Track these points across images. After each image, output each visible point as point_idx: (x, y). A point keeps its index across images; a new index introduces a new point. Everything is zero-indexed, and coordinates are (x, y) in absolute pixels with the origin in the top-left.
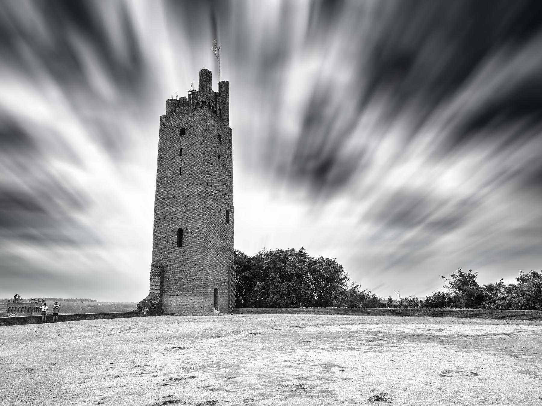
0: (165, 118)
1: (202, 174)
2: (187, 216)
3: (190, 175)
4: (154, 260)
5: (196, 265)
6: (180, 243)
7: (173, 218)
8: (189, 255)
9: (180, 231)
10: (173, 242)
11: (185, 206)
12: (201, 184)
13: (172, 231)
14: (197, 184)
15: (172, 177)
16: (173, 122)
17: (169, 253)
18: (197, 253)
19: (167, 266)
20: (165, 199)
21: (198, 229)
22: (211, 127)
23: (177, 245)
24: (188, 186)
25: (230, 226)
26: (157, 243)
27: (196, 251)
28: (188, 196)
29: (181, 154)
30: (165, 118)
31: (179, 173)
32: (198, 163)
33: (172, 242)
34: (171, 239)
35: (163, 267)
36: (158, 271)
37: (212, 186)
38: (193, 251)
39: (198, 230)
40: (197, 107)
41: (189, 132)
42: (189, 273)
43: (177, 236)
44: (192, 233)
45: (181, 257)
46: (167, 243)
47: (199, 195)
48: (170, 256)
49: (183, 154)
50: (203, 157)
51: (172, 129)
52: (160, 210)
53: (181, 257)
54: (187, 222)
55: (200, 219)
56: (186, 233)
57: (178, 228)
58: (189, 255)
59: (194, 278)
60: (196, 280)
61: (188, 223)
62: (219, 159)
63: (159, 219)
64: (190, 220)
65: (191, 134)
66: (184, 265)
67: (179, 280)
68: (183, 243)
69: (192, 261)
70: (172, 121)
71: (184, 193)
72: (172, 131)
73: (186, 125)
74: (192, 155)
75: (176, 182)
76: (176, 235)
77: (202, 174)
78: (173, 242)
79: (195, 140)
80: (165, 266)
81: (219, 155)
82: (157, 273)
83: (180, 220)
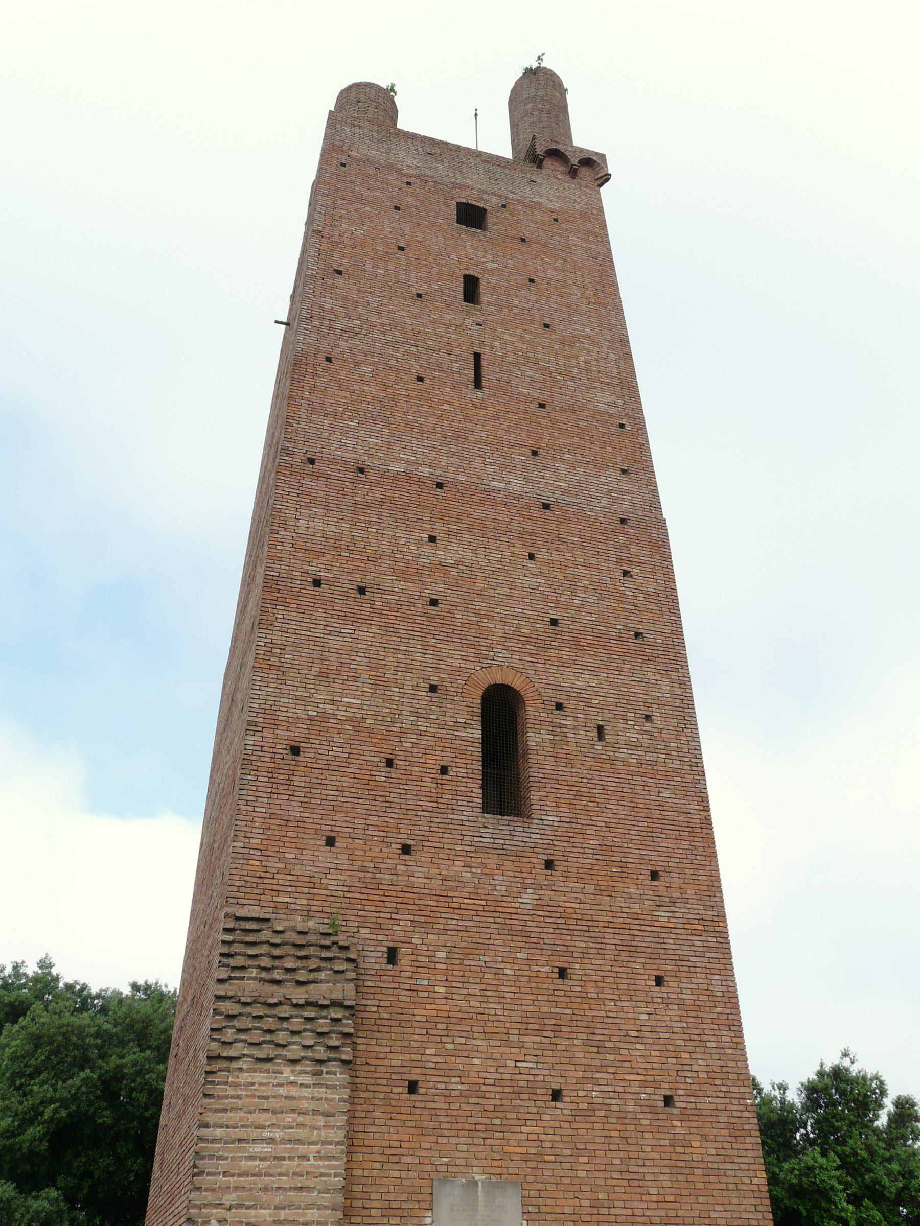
2: (554, 622)
5: (671, 984)
7: (434, 603)
8: (599, 891)
10: (444, 770)
13: (433, 688)
17: (406, 849)
18: (663, 891)
19: (392, 955)
20: (372, 476)
26: (295, 751)
31: (471, 374)
33: (433, 763)
34: (427, 742)
38: (623, 865)
39: (647, 726)
42: (616, 1051)
43: (478, 734)
45: (528, 898)
53: (528, 898)
55: (652, 659)
57: (488, 678)
58: (599, 891)
59: (668, 1101)
60: (685, 1116)
61: (562, 664)
63: (317, 583)
66: (562, 973)
68: (535, 796)
76: (465, 726)
78: (444, 770)
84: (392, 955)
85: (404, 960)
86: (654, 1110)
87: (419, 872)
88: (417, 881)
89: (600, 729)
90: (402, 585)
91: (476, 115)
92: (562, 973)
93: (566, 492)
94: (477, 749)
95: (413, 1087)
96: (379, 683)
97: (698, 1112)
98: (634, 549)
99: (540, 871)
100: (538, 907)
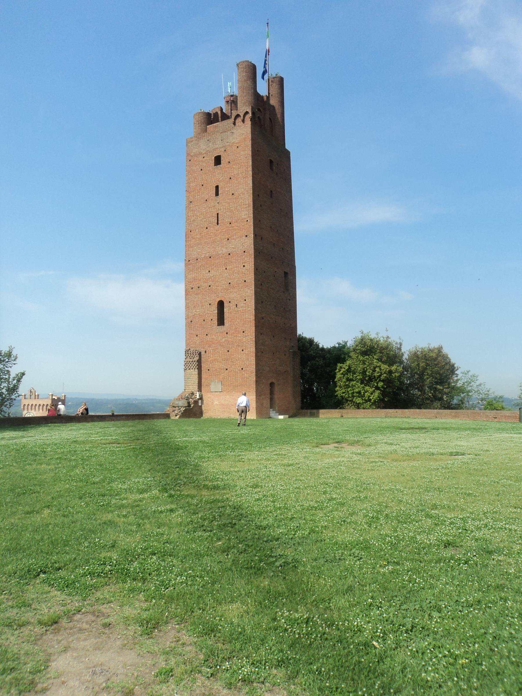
0: (193, 141)
1: (247, 221)
2: (230, 283)
3: (230, 223)
4: (187, 344)
6: (221, 321)
9: (221, 305)
10: (212, 320)
11: (226, 269)
12: (246, 236)
13: (210, 304)
14: (241, 237)
15: (207, 228)
16: (204, 147)
17: (207, 335)
19: (206, 352)
21: (245, 300)
22: (258, 151)
23: (218, 324)
24: (228, 239)
25: (291, 294)
27: (243, 332)
28: (229, 254)
29: (217, 194)
30: (193, 141)
32: (241, 205)
35: (200, 354)
36: (195, 359)
37: (262, 238)
40: (237, 121)
41: (227, 160)
42: (235, 362)
44: (237, 307)
46: (204, 320)
47: (244, 252)
48: (209, 338)
49: (219, 193)
50: (247, 196)
51: (204, 157)
52: (191, 276)
54: (229, 291)
55: (247, 286)
56: (228, 306)
57: (218, 300)
59: (242, 369)
60: (244, 371)
62: (271, 197)
63: (192, 288)
64: (234, 287)
65: (229, 162)
66: (228, 351)
67: (222, 371)
69: (239, 346)
70: (203, 146)
71: (224, 249)
72: (204, 159)
73: (223, 149)
74: (233, 194)
75: (212, 234)
76: (214, 311)
77: (247, 221)
78: (212, 320)
79: (236, 172)
80: (203, 353)
81: (271, 191)
82: (192, 362)
83: (219, 288)
84: (206, 352)
85: (207, 352)
86: (240, 370)
87: (209, 338)
88: (208, 340)
89: (237, 305)
90: (205, 284)
91: (268, 23)
92: (228, 351)
93: (234, 248)
94: (216, 314)
95: (209, 370)
96: (202, 306)
97: (246, 370)
98: (246, 259)
99: (226, 335)
100: (225, 341)
